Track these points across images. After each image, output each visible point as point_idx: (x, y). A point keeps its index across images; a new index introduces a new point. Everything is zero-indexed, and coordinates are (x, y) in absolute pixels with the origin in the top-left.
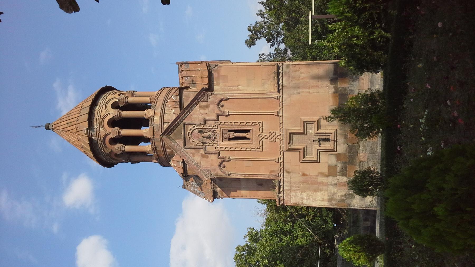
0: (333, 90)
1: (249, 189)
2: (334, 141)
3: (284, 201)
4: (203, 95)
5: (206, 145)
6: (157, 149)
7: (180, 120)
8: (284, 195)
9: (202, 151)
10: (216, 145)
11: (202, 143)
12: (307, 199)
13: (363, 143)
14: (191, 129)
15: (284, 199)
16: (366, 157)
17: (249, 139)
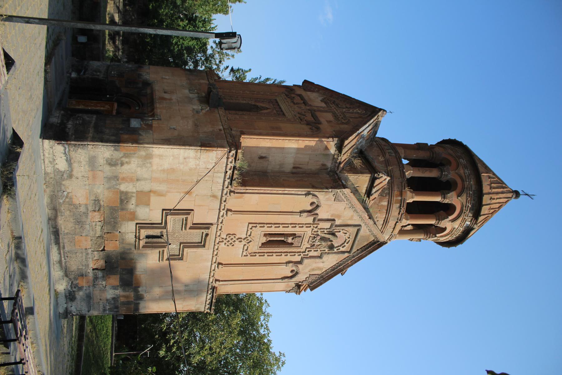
0: (140, 289)
2: (139, 239)
3: (228, 155)
4: (314, 282)
6: (399, 205)
7: (354, 257)
8: (227, 164)
9: (338, 222)
10: (316, 230)
11: (333, 234)
12: (189, 158)
13: (95, 234)
14: (343, 247)
15: (228, 158)
16: (90, 217)
17: (265, 235)
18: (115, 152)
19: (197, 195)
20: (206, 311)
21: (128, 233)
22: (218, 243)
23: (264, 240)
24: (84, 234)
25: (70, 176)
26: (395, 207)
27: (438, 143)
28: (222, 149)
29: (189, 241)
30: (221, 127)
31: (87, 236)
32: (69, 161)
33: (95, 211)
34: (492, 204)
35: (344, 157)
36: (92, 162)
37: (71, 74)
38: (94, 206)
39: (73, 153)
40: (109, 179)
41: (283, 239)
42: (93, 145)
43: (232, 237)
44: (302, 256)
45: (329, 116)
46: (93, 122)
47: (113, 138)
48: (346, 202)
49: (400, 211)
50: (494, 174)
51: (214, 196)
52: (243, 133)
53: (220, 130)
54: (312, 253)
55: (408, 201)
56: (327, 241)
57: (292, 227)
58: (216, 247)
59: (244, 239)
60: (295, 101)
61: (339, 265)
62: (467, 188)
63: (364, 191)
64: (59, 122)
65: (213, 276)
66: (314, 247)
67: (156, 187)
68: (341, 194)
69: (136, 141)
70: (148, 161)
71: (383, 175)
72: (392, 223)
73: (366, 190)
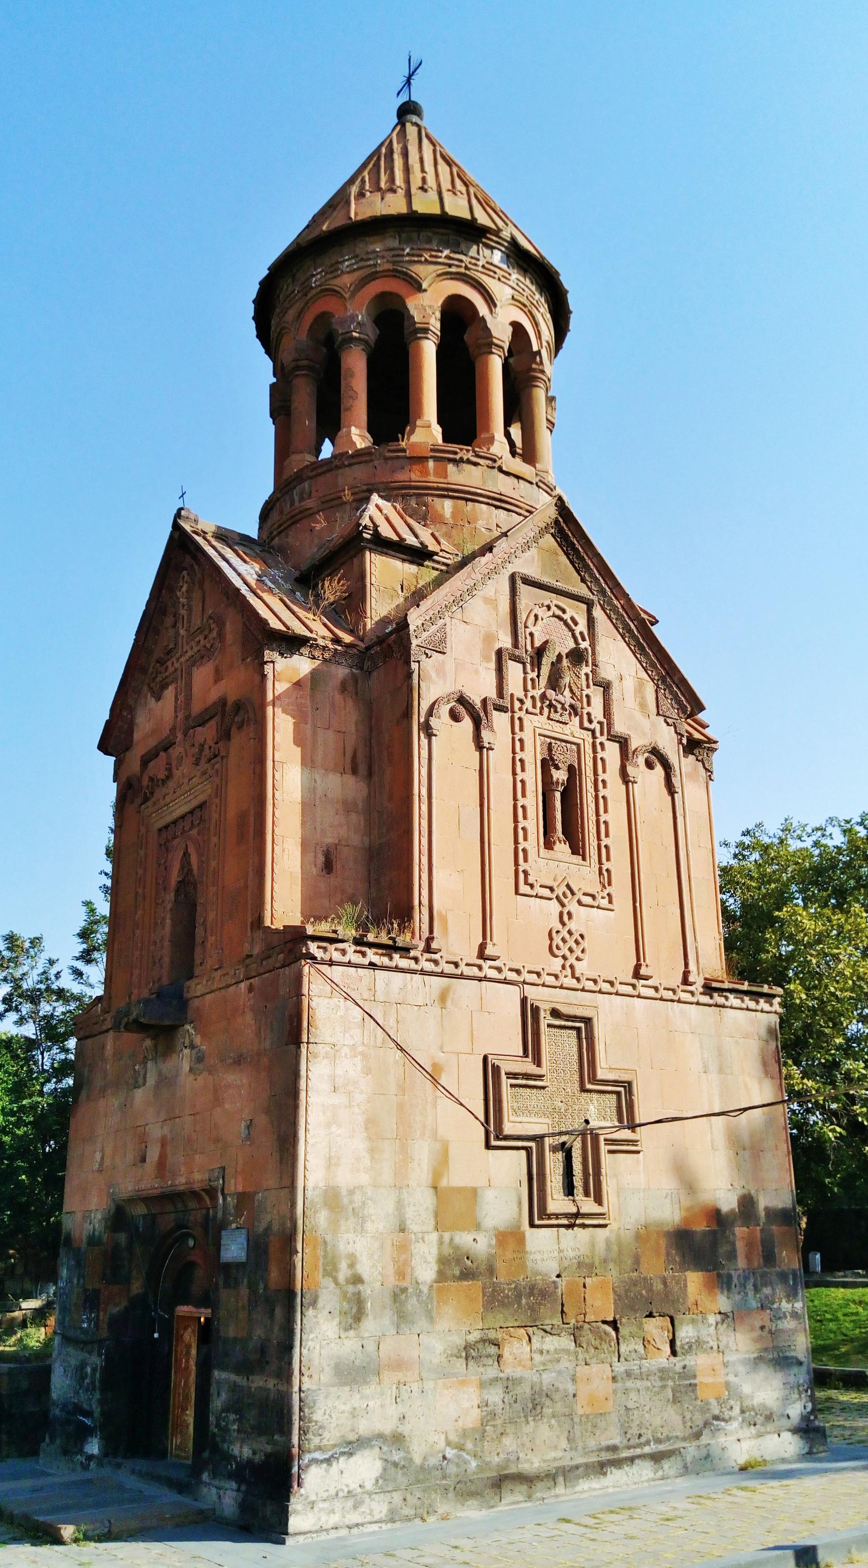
1: (308, 807)
2: (577, 1215)
3: (323, 962)
4: (679, 702)
5: (528, 666)
6: (451, 467)
7: (602, 592)
8: (349, 964)
10: (528, 704)
11: (540, 653)
12: (333, 1078)
13: (567, 1352)
14: (576, 624)
15: (331, 963)
16: (518, 1372)
17: (549, 845)
18: (320, 1303)
19: (441, 1048)
20: (777, 1007)
21: (560, 1251)
22: (578, 980)
23: (562, 848)
24: (571, 1389)
25: (398, 1440)
26: (458, 476)
27: (268, 352)
28: (305, 980)
29: (576, 1067)
30: (242, 985)
31: (574, 1379)
32: (352, 1447)
33: (499, 1356)
34: (439, 186)
35: (318, 629)
36: (352, 1374)
37: (90, 1457)
38: (485, 1361)
39: (326, 1435)
40: (402, 1318)
41: (558, 795)
42: (301, 1374)
43: (557, 940)
44: (603, 739)
45: (202, 675)
46: (233, 1377)
47: (279, 1312)
48: (447, 619)
49: (469, 462)
50: (351, 181)
51: (443, 997)
52: (260, 919)
53: (251, 989)
54: (597, 710)
55: (440, 440)
56: (560, 670)
57: (523, 770)
58: (590, 985)
59: (563, 905)
60: (161, 775)
61: (626, 633)
62: (394, 263)
63: (413, 569)
64: (234, 1485)
65: (674, 991)
66: (578, 704)
67: (420, 1172)
68: (425, 635)
69: (288, 1240)
70: (346, 1201)
71: (367, 514)
72: (503, 485)
73: (412, 562)
